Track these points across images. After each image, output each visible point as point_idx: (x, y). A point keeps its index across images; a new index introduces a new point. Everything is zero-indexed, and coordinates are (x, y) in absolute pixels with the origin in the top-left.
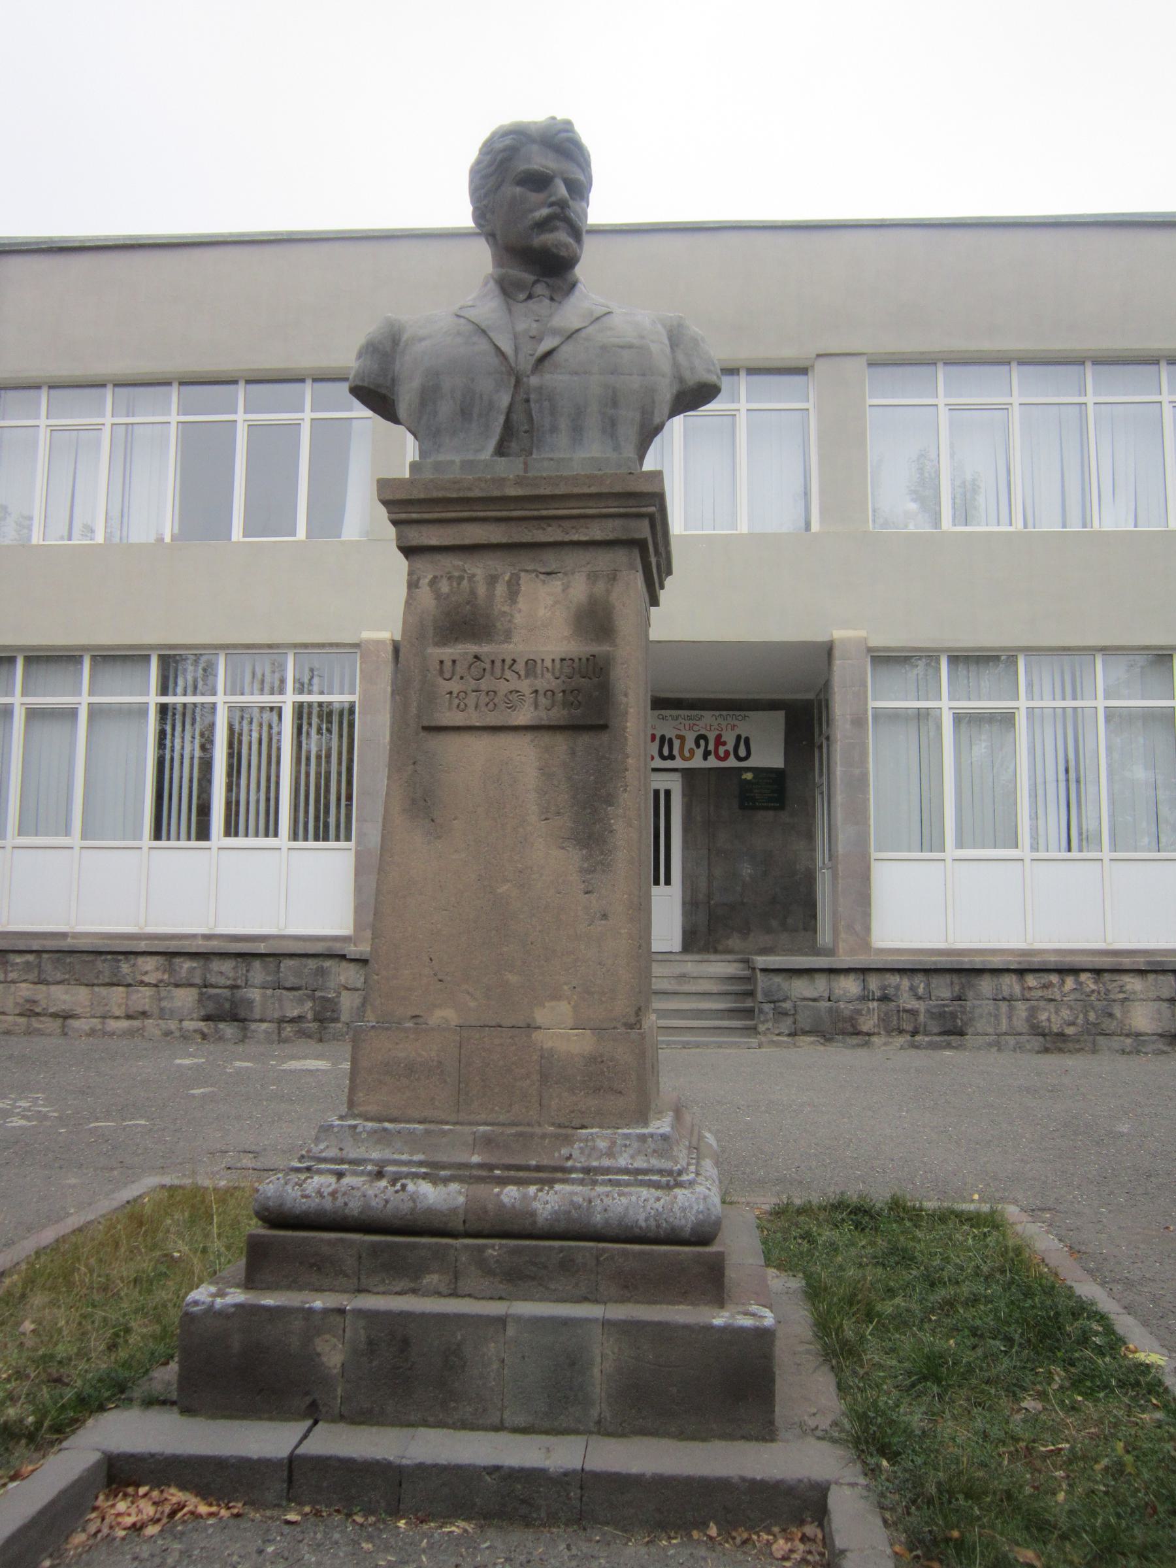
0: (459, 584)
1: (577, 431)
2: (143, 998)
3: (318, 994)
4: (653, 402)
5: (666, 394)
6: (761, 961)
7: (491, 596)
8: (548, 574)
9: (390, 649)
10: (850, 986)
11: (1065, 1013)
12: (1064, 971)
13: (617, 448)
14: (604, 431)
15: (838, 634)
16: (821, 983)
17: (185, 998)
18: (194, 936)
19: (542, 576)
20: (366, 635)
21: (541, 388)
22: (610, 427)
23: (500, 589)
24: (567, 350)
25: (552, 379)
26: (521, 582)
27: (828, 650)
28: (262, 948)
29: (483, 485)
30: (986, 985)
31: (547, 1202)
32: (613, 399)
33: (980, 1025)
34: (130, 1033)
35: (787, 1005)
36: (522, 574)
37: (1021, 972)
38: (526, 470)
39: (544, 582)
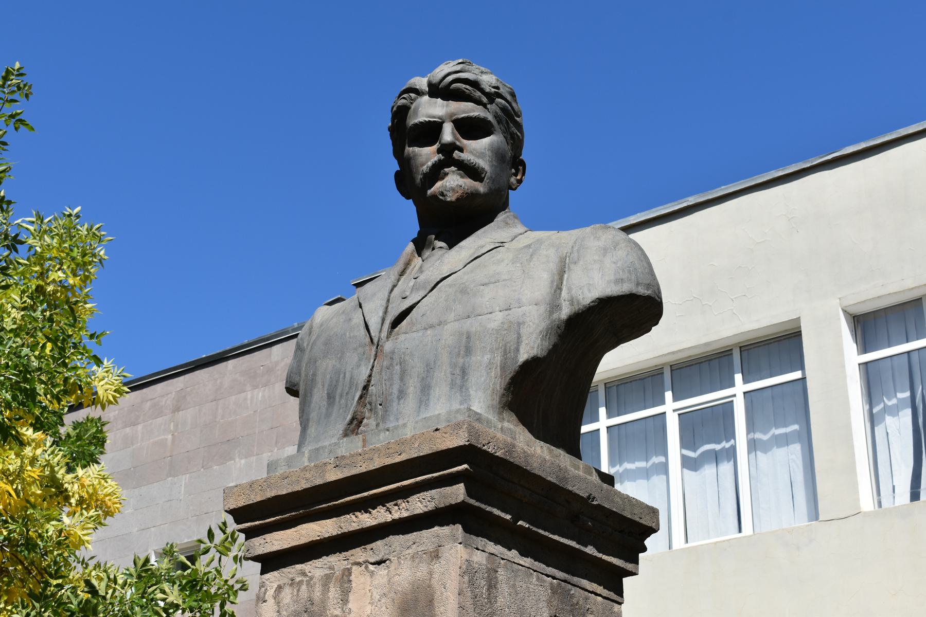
0: (298, 591)
1: (425, 389)
4: (519, 337)
7: (324, 601)
8: (379, 563)
14: (453, 384)
19: (371, 567)
21: (393, 352)
23: (334, 592)
25: (407, 339)
26: (352, 578)
29: (308, 475)
32: (467, 345)
36: (354, 568)
38: (364, 446)
39: (372, 573)
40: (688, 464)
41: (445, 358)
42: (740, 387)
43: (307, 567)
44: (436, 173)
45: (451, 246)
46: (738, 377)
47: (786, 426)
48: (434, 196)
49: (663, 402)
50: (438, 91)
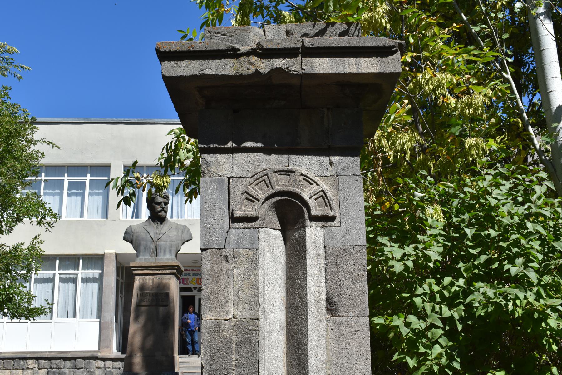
1: (165, 252)
3: (88, 370)
5: (180, 244)
9: (114, 256)
13: (171, 255)
18: (46, 352)
20: (107, 251)
24: (164, 237)
28: (69, 355)
40: (69, 195)
41: (168, 248)
42: (88, 178)
43: (145, 277)
44: (160, 211)
45: (161, 224)
46: (89, 175)
47: (98, 190)
48: (160, 216)
49: (64, 176)
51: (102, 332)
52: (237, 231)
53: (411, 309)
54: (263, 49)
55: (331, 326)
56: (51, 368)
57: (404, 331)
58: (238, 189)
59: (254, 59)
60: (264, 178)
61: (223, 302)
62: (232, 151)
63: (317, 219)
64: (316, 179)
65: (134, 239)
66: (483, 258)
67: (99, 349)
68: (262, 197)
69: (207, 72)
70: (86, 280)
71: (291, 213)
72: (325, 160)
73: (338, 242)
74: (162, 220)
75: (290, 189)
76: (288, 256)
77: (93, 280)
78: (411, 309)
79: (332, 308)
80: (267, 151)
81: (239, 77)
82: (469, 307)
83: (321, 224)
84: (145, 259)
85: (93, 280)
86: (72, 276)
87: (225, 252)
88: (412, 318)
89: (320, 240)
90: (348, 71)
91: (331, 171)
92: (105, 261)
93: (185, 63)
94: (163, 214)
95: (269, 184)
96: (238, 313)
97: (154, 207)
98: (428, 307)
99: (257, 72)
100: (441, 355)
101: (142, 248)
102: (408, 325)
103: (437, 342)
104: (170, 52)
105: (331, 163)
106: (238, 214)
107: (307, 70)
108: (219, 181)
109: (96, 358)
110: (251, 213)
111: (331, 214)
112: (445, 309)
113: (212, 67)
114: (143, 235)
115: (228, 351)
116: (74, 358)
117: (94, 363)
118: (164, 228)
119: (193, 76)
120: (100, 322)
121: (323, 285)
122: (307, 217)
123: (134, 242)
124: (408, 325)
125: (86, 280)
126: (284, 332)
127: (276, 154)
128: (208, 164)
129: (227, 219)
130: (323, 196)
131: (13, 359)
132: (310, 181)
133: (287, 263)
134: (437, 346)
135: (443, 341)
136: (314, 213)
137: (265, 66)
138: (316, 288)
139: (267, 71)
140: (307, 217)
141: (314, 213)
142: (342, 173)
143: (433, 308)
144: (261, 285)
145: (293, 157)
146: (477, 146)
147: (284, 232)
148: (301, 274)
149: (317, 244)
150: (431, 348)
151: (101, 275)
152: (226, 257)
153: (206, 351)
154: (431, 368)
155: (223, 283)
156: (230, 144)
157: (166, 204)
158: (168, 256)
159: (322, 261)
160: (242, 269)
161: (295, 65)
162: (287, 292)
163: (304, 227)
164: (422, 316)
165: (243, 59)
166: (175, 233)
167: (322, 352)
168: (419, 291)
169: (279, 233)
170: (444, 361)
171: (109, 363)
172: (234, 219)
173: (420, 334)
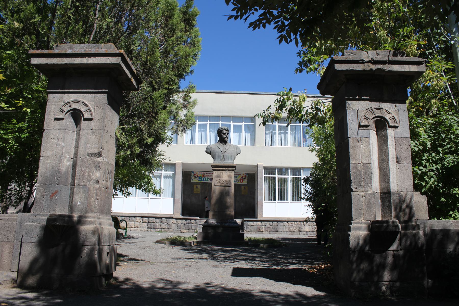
1: (228, 159)
2: (137, 224)
6: (245, 219)
10: (260, 223)
11: (295, 228)
12: (294, 221)
15: (259, 164)
16: (254, 223)
17: (145, 224)
20: (177, 162)
22: (231, 159)
24: (227, 151)
27: (257, 166)
28: (158, 216)
30: (282, 223)
31: (227, 225)
33: (280, 230)
34: (135, 230)
35: (249, 227)
37: (287, 221)
44: (225, 138)
50: (225, 130)
51: (175, 204)
52: (362, 131)
53: (421, 164)
54: (373, 61)
55: (398, 167)
56: (149, 222)
57: (419, 172)
58: (362, 114)
59: (370, 64)
60: (371, 111)
61: (358, 157)
62: (359, 100)
63: (392, 127)
64: (391, 112)
65: (212, 152)
66: (449, 146)
67: (174, 213)
68: (371, 118)
69: (352, 69)
70: (165, 177)
71: (381, 125)
72: (394, 105)
73: (399, 136)
74: (225, 142)
75: (381, 115)
76: (378, 141)
77: (170, 177)
78: (421, 164)
79: (398, 161)
80: (371, 100)
81: (365, 71)
82: (443, 165)
83: (393, 129)
84: (219, 162)
85: (170, 177)
86: (158, 174)
87: (357, 138)
88: (421, 168)
89: (393, 135)
90: (405, 70)
91: (396, 109)
92: (177, 167)
93: (344, 65)
94: (226, 139)
95: (373, 113)
96: (363, 161)
97: (222, 136)
98: (427, 164)
99: (371, 69)
100: (435, 181)
101: (216, 157)
102: (420, 170)
103: (432, 177)
104: (338, 60)
105: (396, 106)
106: (362, 124)
107: (390, 69)
108: (354, 112)
109: (172, 218)
110: (367, 124)
111: (397, 125)
112: (434, 165)
113: (354, 67)
114: (217, 150)
115: (360, 175)
116: (161, 218)
117: (171, 220)
118: (227, 146)
119: (347, 70)
120: (174, 199)
121: (395, 152)
122: (387, 126)
123: (212, 153)
124: (420, 170)
125: (166, 177)
126: (378, 169)
127: (375, 102)
128: (349, 105)
129: (357, 126)
130: (394, 118)
131: (129, 217)
132: (388, 112)
133: (378, 144)
134: (432, 178)
135: (434, 176)
136: (390, 125)
137: (374, 67)
138: (392, 153)
139: (375, 69)
140: (387, 126)
141: (390, 125)
142: (400, 110)
143: (429, 165)
144: (371, 151)
145: (381, 103)
146: (436, 103)
147: (377, 132)
148: (385, 148)
149: (392, 137)
150: (430, 178)
151: (174, 175)
152: (358, 140)
153: (352, 175)
154: (431, 186)
155: (357, 150)
156: (357, 97)
157: (228, 134)
158: (230, 161)
159: (394, 143)
160: (364, 145)
161: (386, 67)
162: (379, 155)
163: (386, 130)
164: (425, 167)
165: (366, 64)
166: (233, 149)
167: (395, 176)
168: (424, 158)
169: (375, 132)
170: (436, 183)
171: (179, 221)
172: (360, 126)
173: (425, 173)
